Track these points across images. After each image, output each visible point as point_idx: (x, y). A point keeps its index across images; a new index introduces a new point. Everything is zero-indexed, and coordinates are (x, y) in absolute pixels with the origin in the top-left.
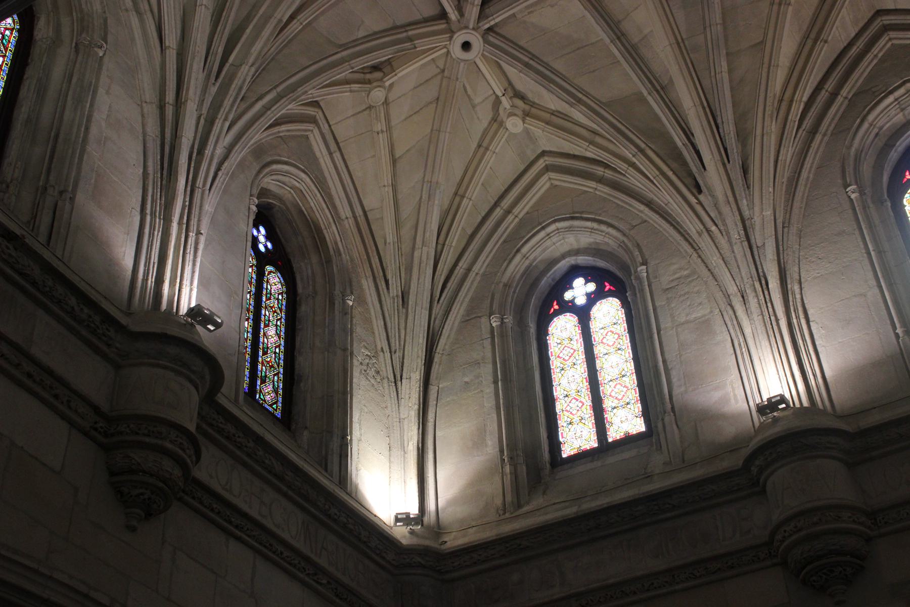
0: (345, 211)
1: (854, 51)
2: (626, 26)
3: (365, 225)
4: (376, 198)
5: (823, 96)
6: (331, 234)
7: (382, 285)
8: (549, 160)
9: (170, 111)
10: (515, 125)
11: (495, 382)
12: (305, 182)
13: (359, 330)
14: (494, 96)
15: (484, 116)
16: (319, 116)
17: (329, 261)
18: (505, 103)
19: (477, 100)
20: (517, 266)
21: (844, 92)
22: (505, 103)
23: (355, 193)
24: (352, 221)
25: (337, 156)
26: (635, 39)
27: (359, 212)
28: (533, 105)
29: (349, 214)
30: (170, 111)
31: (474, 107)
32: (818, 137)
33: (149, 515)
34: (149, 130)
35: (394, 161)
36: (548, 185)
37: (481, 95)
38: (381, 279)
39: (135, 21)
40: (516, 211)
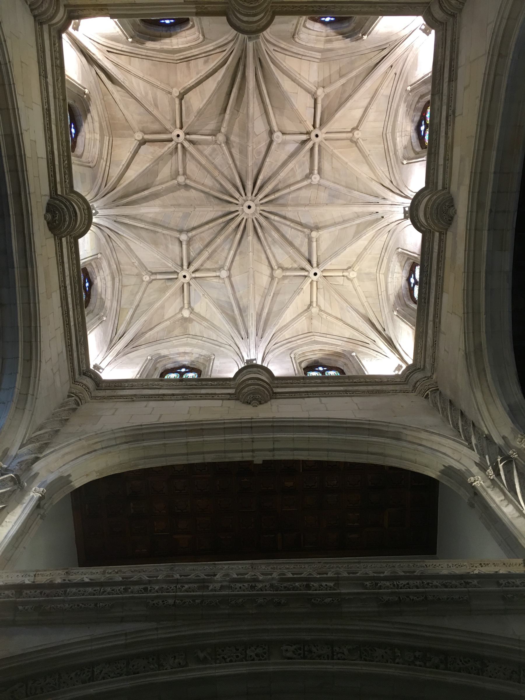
0: (340, 343)
1: (386, 147)
2: (337, 221)
3: (351, 340)
4: (348, 333)
5: (389, 163)
6: (339, 350)
7: (367, 345)
8: (378, 271)
9: (239, 352)
10: (352, 274)
11: (403, 321)
12: (319, 347)
13: (360, 356)
14: (345, 278)
15: (347, 283)
16: (315, 334)
17: (345, 355)
18: (345, 274)
19: (342, 283)
20: (392, 298)
21: (391, 155)
22: (345, 274)
23: (341, 337)
24: (344, 342)
25: (328, 336)
26: (341, 220)
27: (345, 339)
28: (352, 265)
29: (342, 342)
30: (239, 352)
31: (343, 285)
32: (394, 169)
33: (261, 404)
34: (236, 359)
35: (341, 320)
36: (383, 276)
37: (341, 280)
38: (364, 344)
39: (222, 349)
40: (382, 290)
